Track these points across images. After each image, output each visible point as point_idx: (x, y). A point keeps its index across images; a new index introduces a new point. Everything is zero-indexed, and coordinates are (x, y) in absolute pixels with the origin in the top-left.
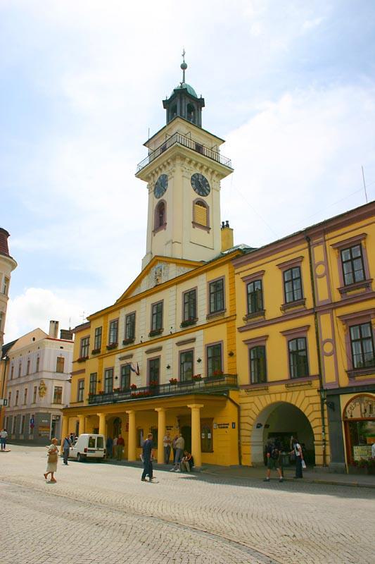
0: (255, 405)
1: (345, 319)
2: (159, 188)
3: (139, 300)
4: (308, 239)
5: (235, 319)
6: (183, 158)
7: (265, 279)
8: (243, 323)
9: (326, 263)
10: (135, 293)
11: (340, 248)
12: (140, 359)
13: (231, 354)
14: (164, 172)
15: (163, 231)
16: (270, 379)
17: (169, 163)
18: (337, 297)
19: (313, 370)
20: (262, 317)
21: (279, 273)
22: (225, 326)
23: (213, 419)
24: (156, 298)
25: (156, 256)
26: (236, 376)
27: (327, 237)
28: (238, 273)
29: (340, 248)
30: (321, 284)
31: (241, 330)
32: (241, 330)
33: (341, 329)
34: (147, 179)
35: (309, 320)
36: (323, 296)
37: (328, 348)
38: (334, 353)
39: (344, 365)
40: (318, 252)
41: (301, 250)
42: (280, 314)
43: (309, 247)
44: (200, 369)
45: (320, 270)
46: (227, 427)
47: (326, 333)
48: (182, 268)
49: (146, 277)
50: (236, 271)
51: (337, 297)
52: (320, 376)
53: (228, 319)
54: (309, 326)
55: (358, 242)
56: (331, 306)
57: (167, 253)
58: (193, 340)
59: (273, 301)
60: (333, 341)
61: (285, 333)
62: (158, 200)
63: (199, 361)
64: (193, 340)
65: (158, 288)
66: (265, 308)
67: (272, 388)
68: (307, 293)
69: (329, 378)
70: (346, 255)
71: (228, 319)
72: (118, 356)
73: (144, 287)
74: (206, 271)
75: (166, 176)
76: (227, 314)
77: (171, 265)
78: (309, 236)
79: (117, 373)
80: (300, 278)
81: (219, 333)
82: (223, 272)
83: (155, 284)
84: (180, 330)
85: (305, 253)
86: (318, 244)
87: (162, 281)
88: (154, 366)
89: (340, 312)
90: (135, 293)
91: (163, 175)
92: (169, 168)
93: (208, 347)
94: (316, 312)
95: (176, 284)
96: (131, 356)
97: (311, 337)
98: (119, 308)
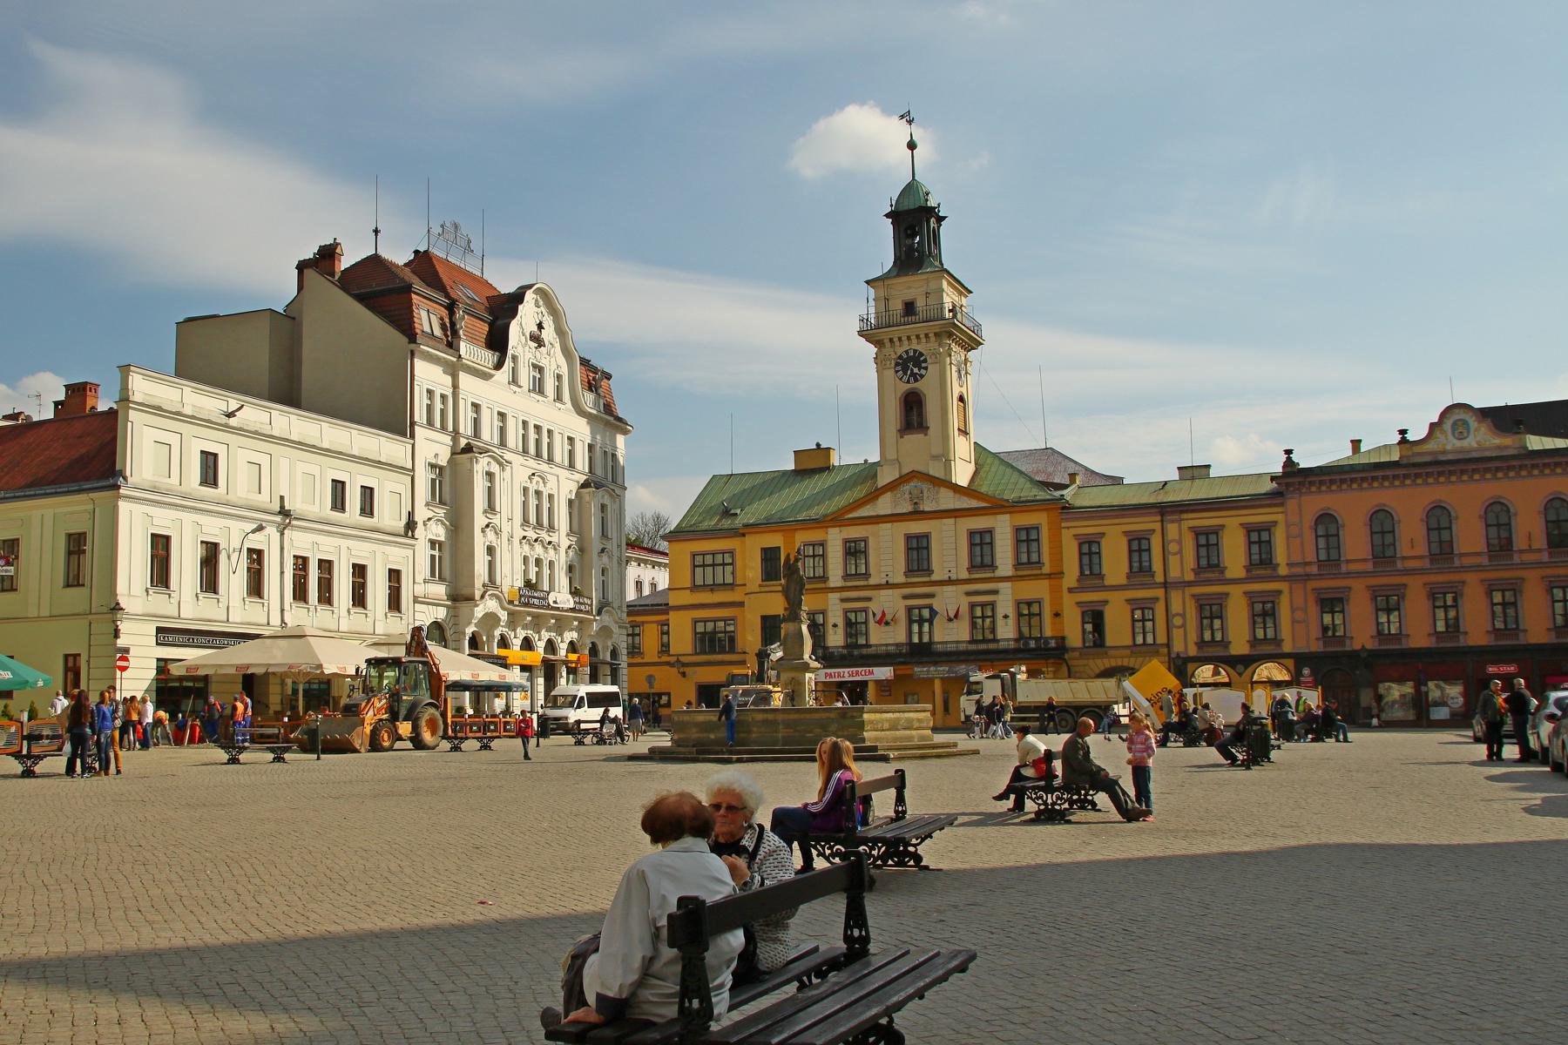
1: (1197, 598)
2: (911, 364)
6: (950, 335)
7: (1104, 542)
8: (1075, 585)
9: (1180, 542)
10: (866, 511)
11: (1197, 532)
12: (889, 602)
13: (1057, 615)
14: (920, 348)
15: (921, 436)
18: (1190, 576)
21: (1124, 541)
22: (1045, 583)
24: (916, 527)
26: (1063, 638)
27: (1185, 516)
29: (1197, 532)
30: (1173, 561)
32: (1070, 590)
34: (878, 343)
35: (1160, 593)
36: (1174, 573)
37: (1177, 621)
38: (1183, 626)
39: (1193, 637)
40: (1172, 529)
41: (1150, 523)
42: (1124, 581)
45: (1173, 547)
47: (1176, 606)
51: (1190, 576)
52: (1168, 645)
54: (1157, 599)
55: (1216, 531)
57: (935, 470)
58: (996, 592)
59: (1115, 563)
60: (1183, 616)
63: (1006, 617)
64: (996, 592)
65: (917, 514)
66: (1104, 572)
67: (1111, 652)
68: (1157, 566)
69: (1178, 647)
72: (834, 598)
73: (884, 506)
75: (921, 354)
76: (1046, 569)
77: (943, 490)
78: (1166, 510)
79: (835, 616)
80: (1149, 550)
81: (1038, 589)
82: (1039, 518)
83: (910, 509)
84: (965, 575)
86: (1172, 521)
88: (920, 616)
90: (866, 511)
93: (1018, 603)
94: (1165, 585)
96: (869, 599)
97: (1160, 609)
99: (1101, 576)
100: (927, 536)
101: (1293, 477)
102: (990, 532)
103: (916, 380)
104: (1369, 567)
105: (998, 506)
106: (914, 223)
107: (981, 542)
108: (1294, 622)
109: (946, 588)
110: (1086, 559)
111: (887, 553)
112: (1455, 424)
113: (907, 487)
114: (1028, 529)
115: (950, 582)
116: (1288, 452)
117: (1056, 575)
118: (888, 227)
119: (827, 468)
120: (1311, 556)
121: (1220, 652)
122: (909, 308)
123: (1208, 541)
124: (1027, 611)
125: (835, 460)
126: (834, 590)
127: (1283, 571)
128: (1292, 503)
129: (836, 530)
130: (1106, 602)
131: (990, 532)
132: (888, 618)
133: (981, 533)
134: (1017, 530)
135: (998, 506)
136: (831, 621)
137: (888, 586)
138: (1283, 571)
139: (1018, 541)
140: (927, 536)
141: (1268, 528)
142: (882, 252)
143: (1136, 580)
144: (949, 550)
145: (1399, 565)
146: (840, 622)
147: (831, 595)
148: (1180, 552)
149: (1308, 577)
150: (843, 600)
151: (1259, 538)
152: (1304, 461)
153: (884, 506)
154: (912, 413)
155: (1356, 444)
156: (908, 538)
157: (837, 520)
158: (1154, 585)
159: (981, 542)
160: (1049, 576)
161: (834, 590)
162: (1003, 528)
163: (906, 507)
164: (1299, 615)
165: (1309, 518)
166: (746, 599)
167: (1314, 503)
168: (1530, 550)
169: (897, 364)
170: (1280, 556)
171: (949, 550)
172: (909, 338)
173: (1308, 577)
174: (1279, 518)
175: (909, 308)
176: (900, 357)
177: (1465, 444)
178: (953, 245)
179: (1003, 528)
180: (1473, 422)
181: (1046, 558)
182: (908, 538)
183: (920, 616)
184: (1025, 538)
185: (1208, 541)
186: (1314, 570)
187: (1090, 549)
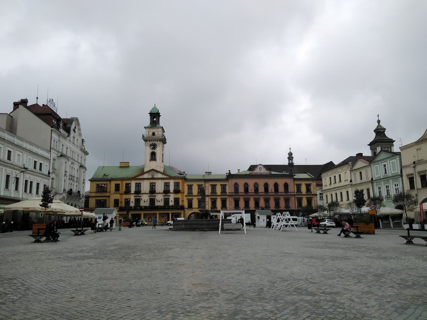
0: (188, 212)
9: (208, 187)
11: (212, 185)
13: (183, 201)
14: (156, 143)
16: (193, 206)
17: (157, 141)
18: (210, 194)
21: (197, 187)
31: (186, 196)
32: (186, 196)
33: (210, 200)
38: (208, 204)
40: (207, 185)
44: (171, 203)
51: (210, 194)
55: (215, 185)
56: (208, 196)
57: (158, 169)
60: (208, 202)
61: (197, 199)
70: (213, 187)
73: (146, 176)
78: (206, 181)
81: (179, 196)
82: (180, 181)
88: (152, 201)
89: (210, 197)
92: (159, 142)
99: (192, 193)
101: (230, 176)
102: (169, 183)
104: (244, 194)
105: (171, 178)
106: (155, 116)
107: (167, 185)
108: (230, 204)
111: (145, 186)
112: (259, 168)
113: (151, 172)
114: (177, 183)
115: (159, 193)
116: (230, 171)
118: (149, 117)
119: (128, 167)
120: (233, 191)
121: (215, 209)
122: (154, 134)
123: (214, 187)
124: (177, 200)
125: (131, 165)
126: (132, 194)
127: (228, 194)
128: (230, 181)
130: (193, 199)
131: (169, 183)
133: (167, 183)
134: (175, 183)
136: (131, 201)
137: (145, 193)
138: (228, 194)
139: (175, 185)
140: (155, 183)
141: (225, 185)
142: (147, 121)
144: (160, 186)
145: (249, 194)
146: (134, 201)
148: (208, 189)
149: (233, 195)
151: (224, 187)
152: (232, 173)
153: (146, 176)
154: (153, 156)
155: (239, 170)
156: (151, 183)
157: (134, 178)
159: (167, 185)
160: (182, 193)
161: (132, 194)
162: (172, 183)
163: (150, 177)
164: (230, 203)
165: (233, 184)
166: (111, 195)
167: (233, 181)
168: (272, 192)
170: (227, 191)
171: (160, 186)
173: (233, 195)
174: (227, 183)
175: (154, 134)
177: (261, 172)
178: (162, 122)
179: (172, 183)
180: (262, 168)
181: (181, 189)
182: (151, 183)
183: (152, 201)
184: (177, 185)
185: (214, 187)
186: (234, 194)
187: (190, 187)
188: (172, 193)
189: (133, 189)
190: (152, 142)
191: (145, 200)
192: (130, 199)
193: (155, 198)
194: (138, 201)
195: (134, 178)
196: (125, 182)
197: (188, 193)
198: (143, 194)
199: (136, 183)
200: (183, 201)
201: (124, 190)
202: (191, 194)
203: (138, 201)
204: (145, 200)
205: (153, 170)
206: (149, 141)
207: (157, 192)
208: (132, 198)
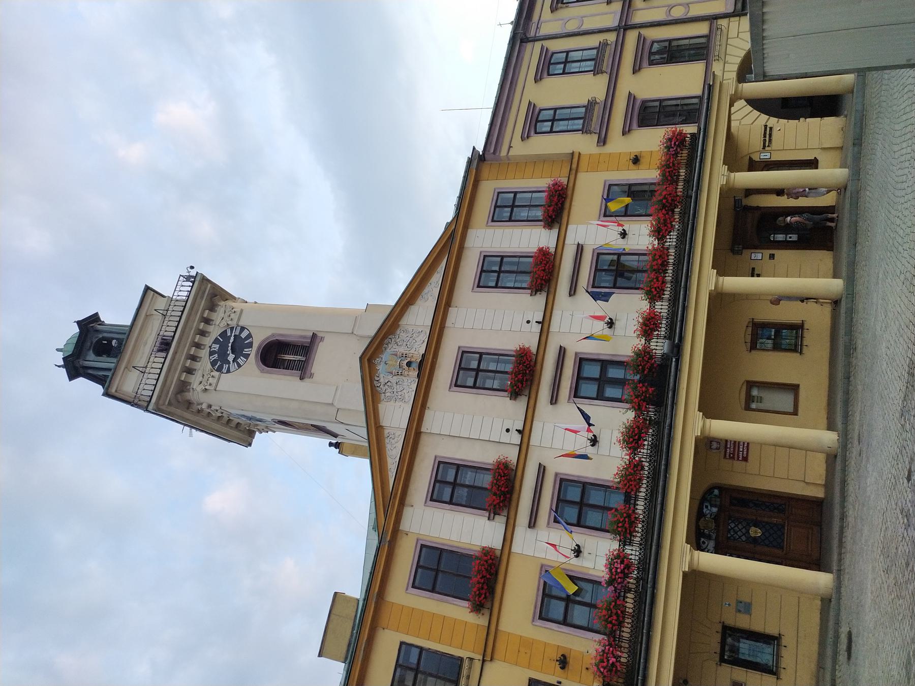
3: (418, 434)
4: (525, 40)
5: (580, 154)
8: (595, 137)
14: (215, 332)
17: (207, 321)
19: (702, 29)
20: (597, 107)
21: (548, 81)
23: (750, 159)
25: (361, 358)
27: (535, 18)
28: (510, 147)
43: (535, 40)
45: (572, 27)
46: (771, 128)
48: (426, 290)
49: (382, 407)
50: (503, 153)
52: (713, 19)
53: (574, 166)
58: (580, 249)
61: (636, 70)
62: (252, 363)
64: (580, 249)
65: (425, 368)
71: (574, 166)
74: (466, 227)
85: (538, 45)
87: (419, 349)
88: (596, 378)
91: (216, 341)
93: (606, 214)
94: (624, 27)
95: (448, 304)
98: (396, 531)
100: (464, 353)
103: (250, 345)
107: (497, 272)
109: (554, 327)
110: (561, 125)
113: (383, 375)
115: (545, 324)
117: (573, 162)
129: (407, 512)
132: (581, 443)
135: (451, 243)
143: (606, 65)
147: (516, 548)
150: (532, 524)
156: (457, 384)
158: (620, 45)
163: (409, 384)
169: (220, 370)
171: (497, 321)
172: (198, 346)
176: (213, 364)
181: (543, 183)
183: (596, 378)
188: (561, 241)
189: (470, 531)
190: (204, 353)
191: (583, 440)
192: (545, 570)
193: (582, 361)
194: (576, 503)
195: (389, 504)
196: (400, 592)
197: (585, 130)
198: (524, 448)
199: (434, 498)
200: (636, 160)
201: (458, 611)
202: (597, 111)
203: (576, 503)
204: (583, 440)
205: (369, 358)
206: (190, 371)
207: (531, 342)
208: (542, 547)
